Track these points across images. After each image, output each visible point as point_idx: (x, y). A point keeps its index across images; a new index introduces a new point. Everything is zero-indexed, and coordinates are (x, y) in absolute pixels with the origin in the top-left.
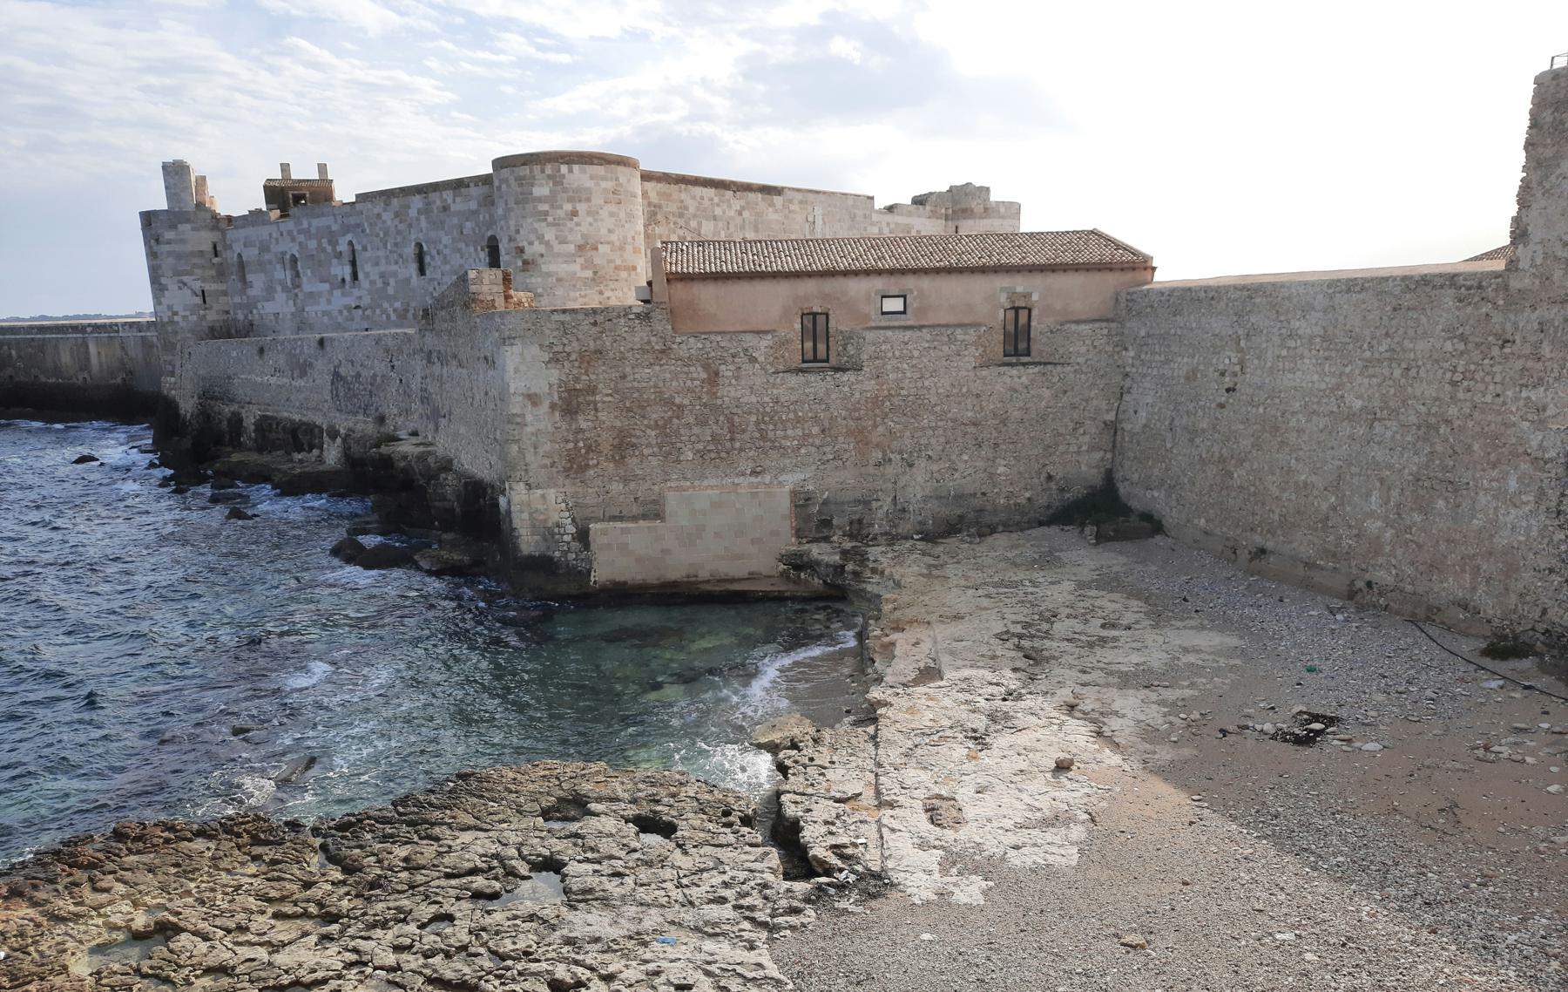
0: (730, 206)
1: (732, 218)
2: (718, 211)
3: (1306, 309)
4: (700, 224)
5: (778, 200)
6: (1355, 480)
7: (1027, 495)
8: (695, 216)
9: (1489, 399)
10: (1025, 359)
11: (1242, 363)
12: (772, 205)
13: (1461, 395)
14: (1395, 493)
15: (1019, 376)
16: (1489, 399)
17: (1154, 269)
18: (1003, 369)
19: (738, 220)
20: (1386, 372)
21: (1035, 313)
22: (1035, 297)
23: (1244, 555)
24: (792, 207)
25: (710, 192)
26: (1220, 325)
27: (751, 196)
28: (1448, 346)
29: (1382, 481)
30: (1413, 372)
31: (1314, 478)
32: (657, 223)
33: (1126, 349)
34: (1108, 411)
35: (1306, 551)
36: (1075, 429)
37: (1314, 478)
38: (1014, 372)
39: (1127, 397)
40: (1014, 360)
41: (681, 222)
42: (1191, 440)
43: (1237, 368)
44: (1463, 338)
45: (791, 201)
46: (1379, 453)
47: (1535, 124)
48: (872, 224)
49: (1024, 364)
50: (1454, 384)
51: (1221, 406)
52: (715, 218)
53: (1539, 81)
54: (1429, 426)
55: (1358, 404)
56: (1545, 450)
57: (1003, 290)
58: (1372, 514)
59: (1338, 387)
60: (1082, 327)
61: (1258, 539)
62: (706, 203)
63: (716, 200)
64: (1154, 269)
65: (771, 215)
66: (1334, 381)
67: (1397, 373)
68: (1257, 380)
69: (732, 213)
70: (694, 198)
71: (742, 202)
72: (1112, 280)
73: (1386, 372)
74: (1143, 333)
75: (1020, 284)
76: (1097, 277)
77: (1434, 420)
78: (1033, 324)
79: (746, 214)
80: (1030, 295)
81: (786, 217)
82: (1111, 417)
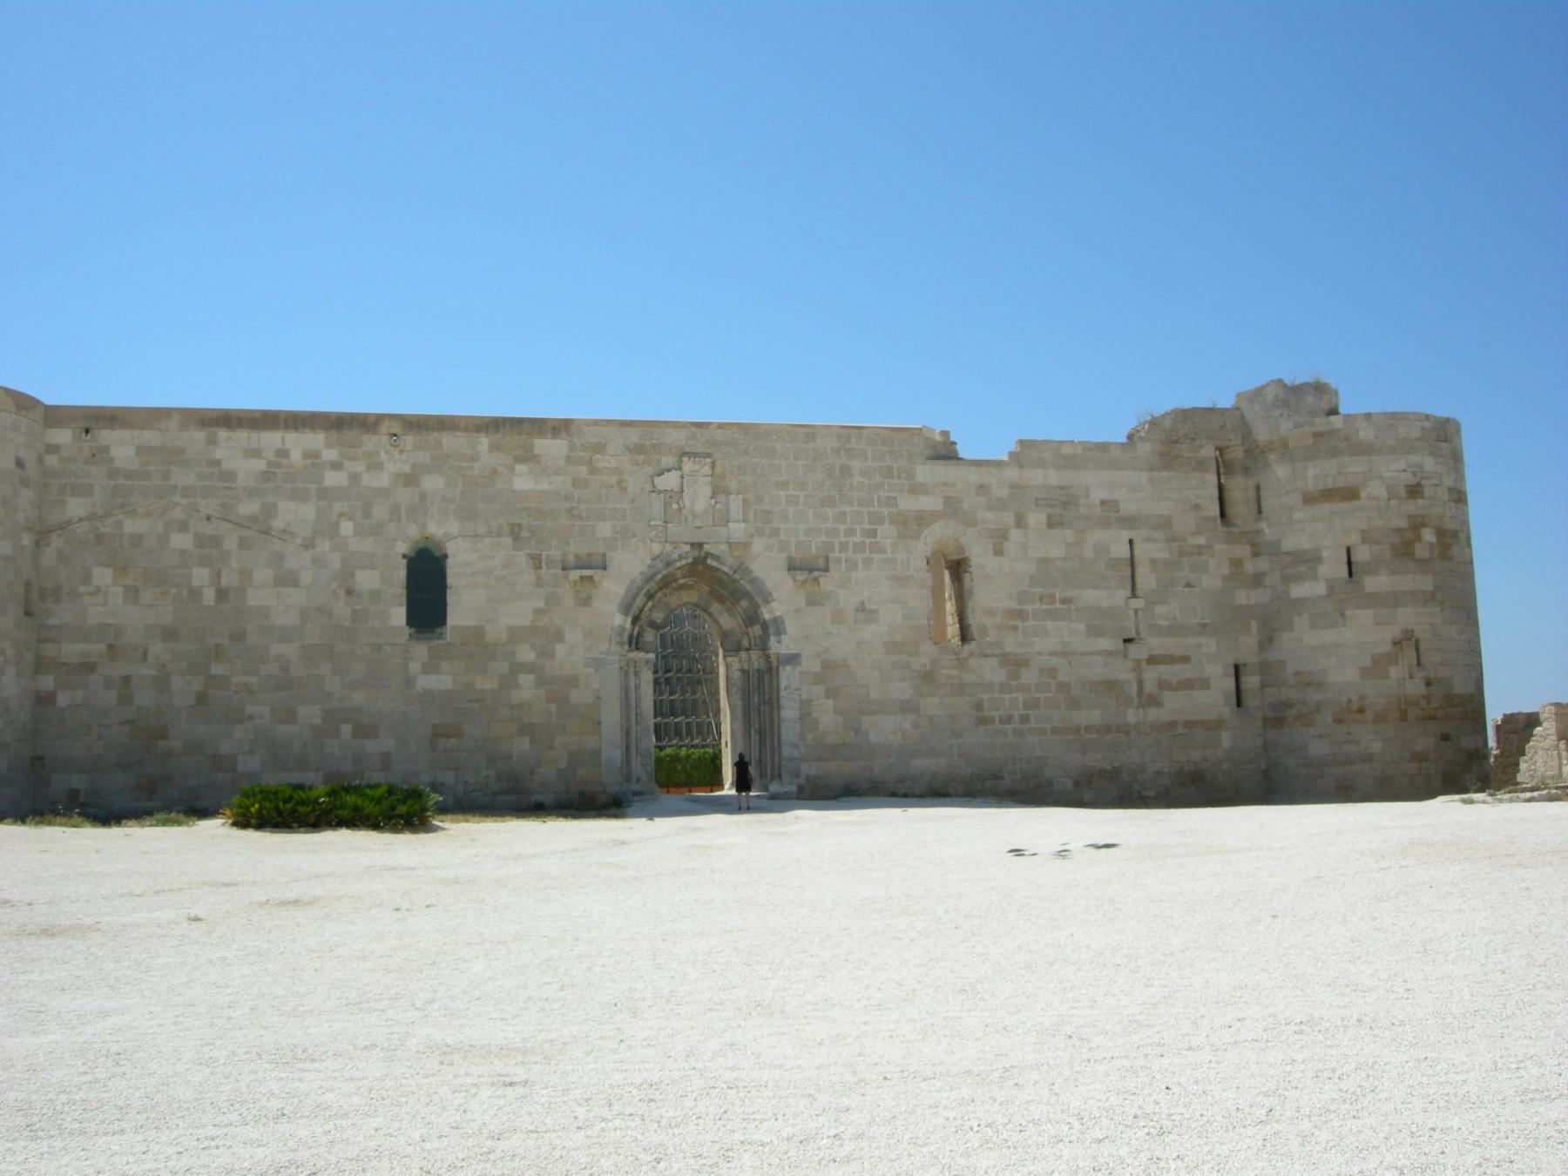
0: (375, 466)
1: (379, 492)
2: (332, 479)
4: (269, 511)
5: (544, 445)
8: (251, 493)
12: (527, 456)
19: (405, 496)
24: (602, 461)
25: (315, 440)
27: (449, 441)
32: (132, 513)
41: (207, 506)
45: (599, 448)
48: (917, 490)
52: (324, 494)
62: (296, 456)
63: (330, 455)
65: (523, 481)
69: (383, 480)
70: (256, 453)
71: (423, 457)
79: (432, 483)
81: (576, 482)
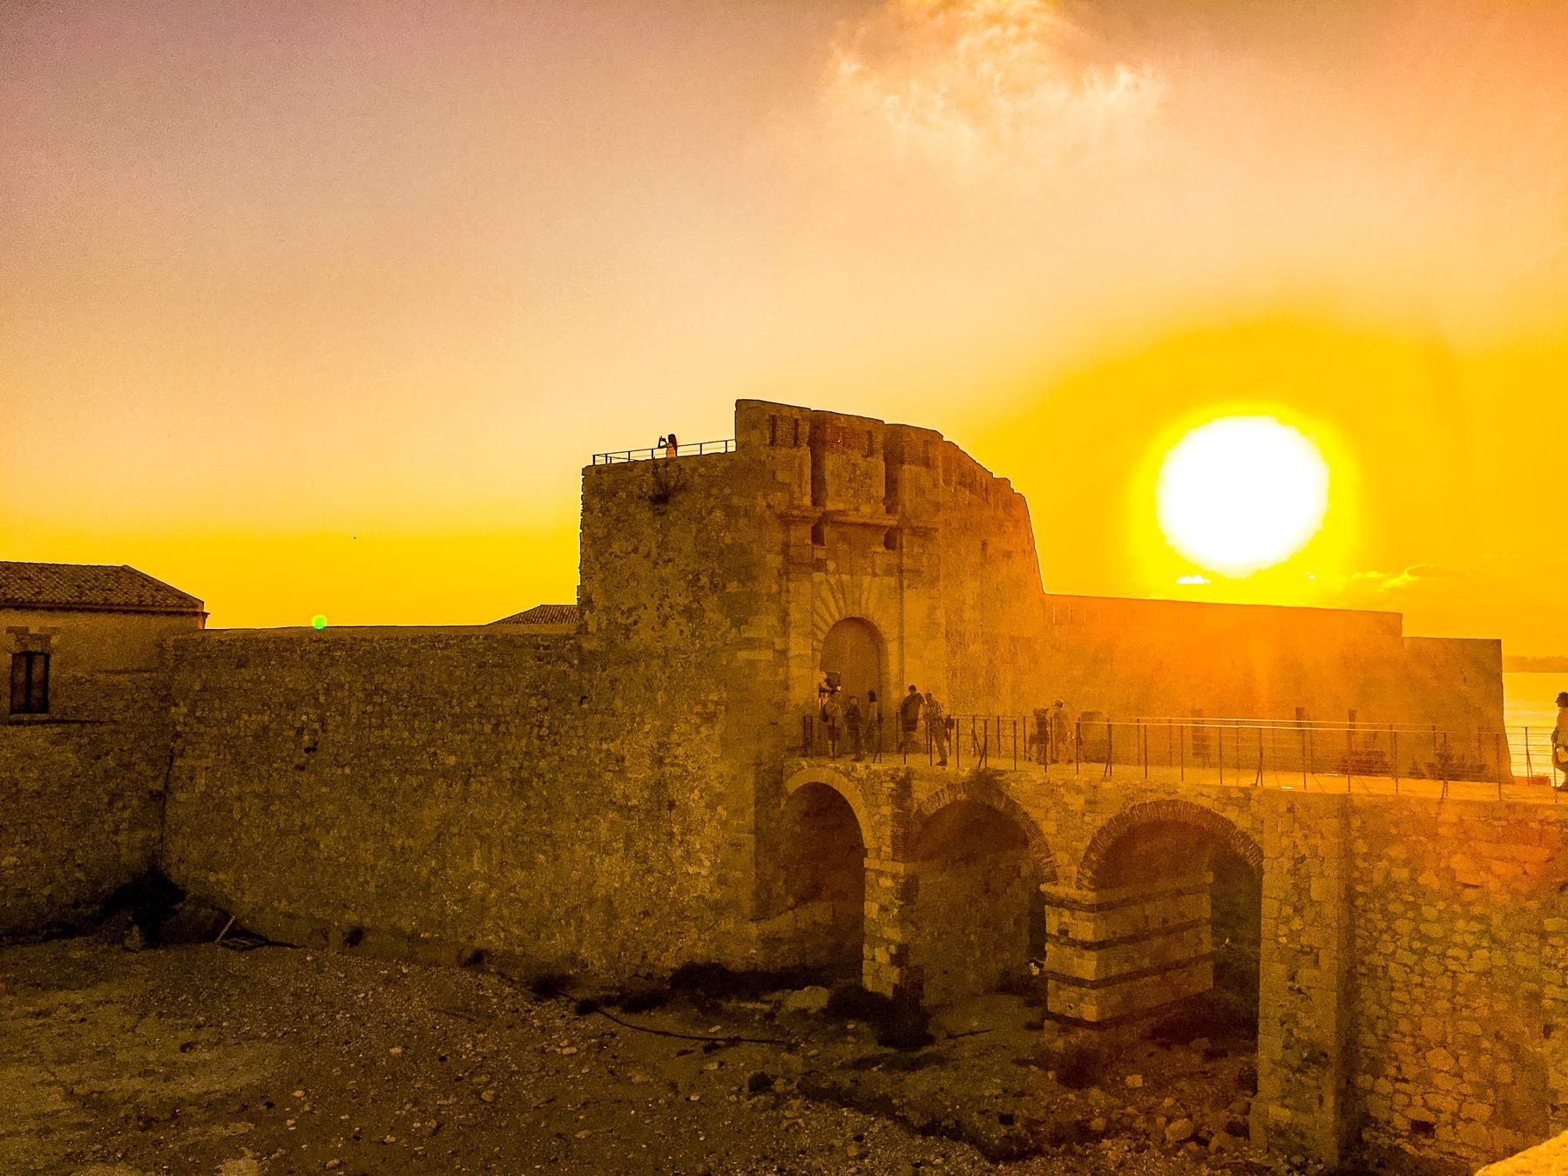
3: (390, 660)
6: (456, 841)
7: (46, 892)
9: (574, 752)
10: (43, 716)
11: (322, 720)
13: (549, 749)
14: (496, 851)
15: (34, 737)
16: (574, 752)
17: (205, 615)
18: (11, 729)
20: (477, 727)
21: (55, 659)
22: (54, 641)
23: (336, 937)
26: (294, 679)
28: (533, 702)
29: (482, 839)
30: (502, 728)
31: (411, 842)
33: (176, 705)
34: (155, 778)
35: (408, 924)
36: (110, 803)
37: (411, 842)
38: (27, 732)
39: (178, 762)
40: (26, 717)
42: (266, 809)
43: (316, 726)
44: (545, 695)
46: (477, 811)
47: (586, 508)
49: (43, 723)
50: (540, 737)
51: (301, 768)
53: (586, 471)
54: (522, 781)
55: (452, 760)
56: (627, 798)
57: (9, 630)
58: (473, 876)
59: (430, 743)
60: (120, 677)
61: (352, 917)
64: (205, 615)
66: (425, 737)
67: (488, 728)
68: (338, 737)
72: (156, 624)
73: (477, 727)
74: (197, 687)
75: (34, 623)
76: (137, 620)
77: (524, 774)
78: (53, 673)
80: (48, 638)
82: (157, 786)
